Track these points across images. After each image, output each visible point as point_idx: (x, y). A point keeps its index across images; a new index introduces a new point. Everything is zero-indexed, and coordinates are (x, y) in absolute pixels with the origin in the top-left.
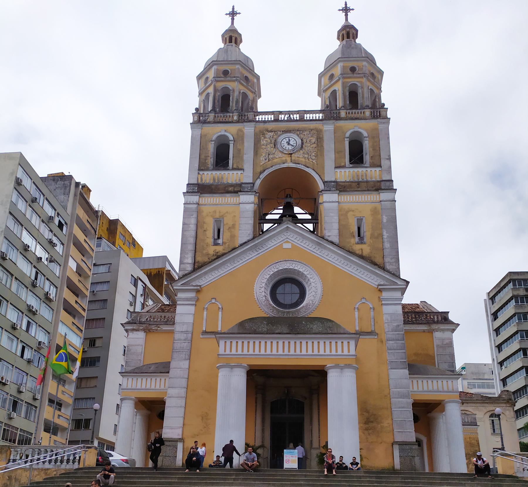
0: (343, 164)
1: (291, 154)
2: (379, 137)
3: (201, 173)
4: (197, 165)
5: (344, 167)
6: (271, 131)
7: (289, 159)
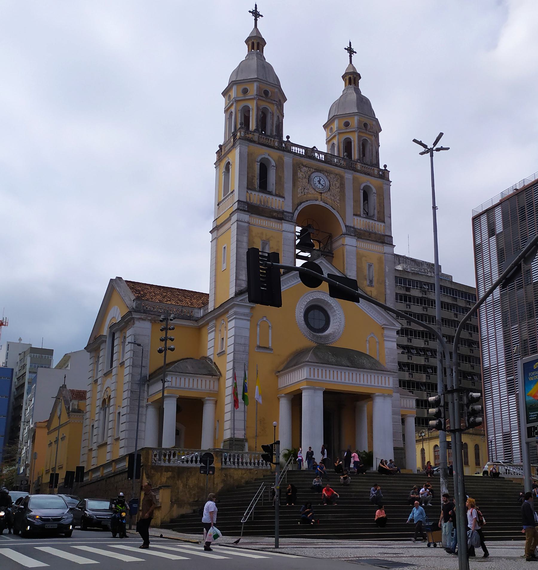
0: (359, 213)
1: (321, 193)
2: (383, 196)
3: (249, 192)
4: (245, 183)
5: (359, 216)
6: (306, 166)
7: (319, 197)
